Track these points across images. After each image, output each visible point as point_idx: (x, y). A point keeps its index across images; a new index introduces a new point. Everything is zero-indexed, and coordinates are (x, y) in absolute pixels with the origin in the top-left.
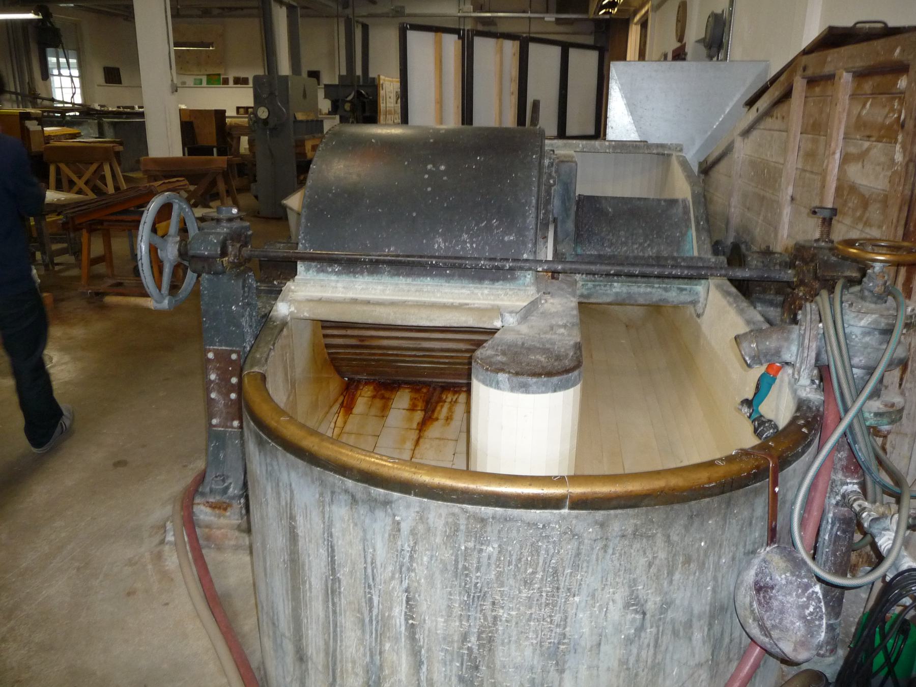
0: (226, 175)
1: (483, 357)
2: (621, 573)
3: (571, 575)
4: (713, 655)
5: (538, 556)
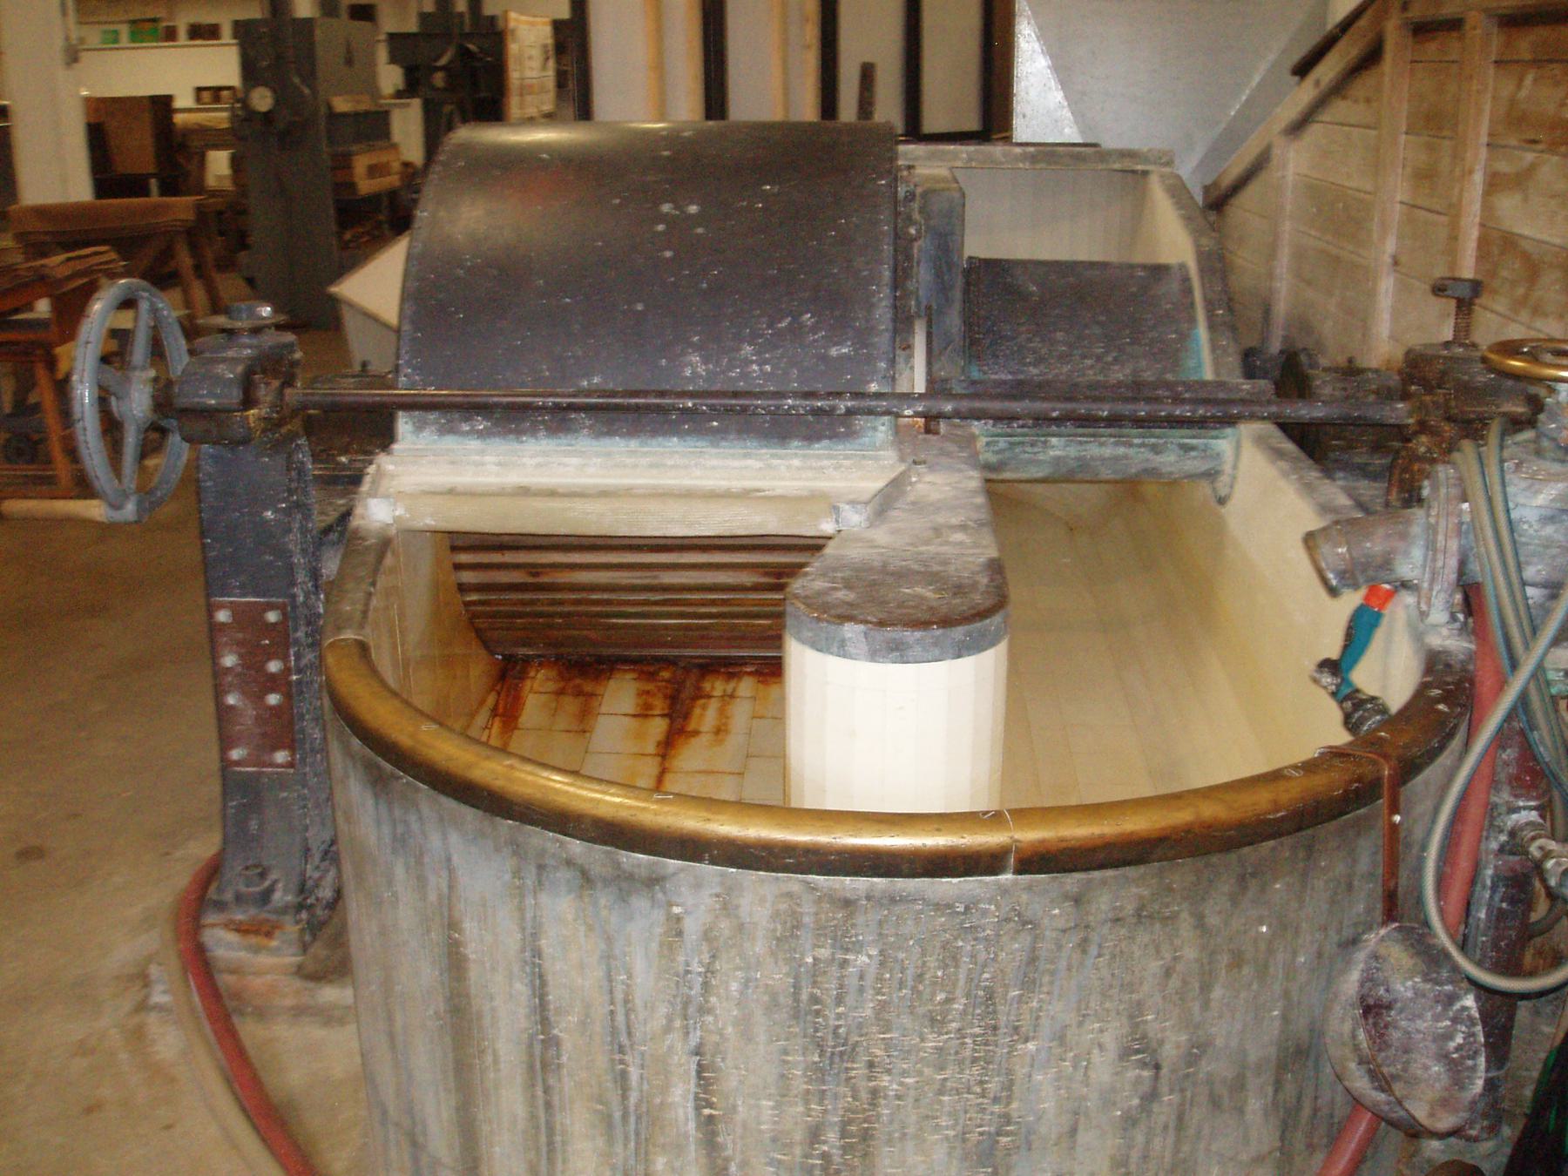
0: (193, 235)
1: (808, 593)
2: (1114, 991)
3: (1019, 1002)
4: (1282, 1139)
5: (957, 967)
